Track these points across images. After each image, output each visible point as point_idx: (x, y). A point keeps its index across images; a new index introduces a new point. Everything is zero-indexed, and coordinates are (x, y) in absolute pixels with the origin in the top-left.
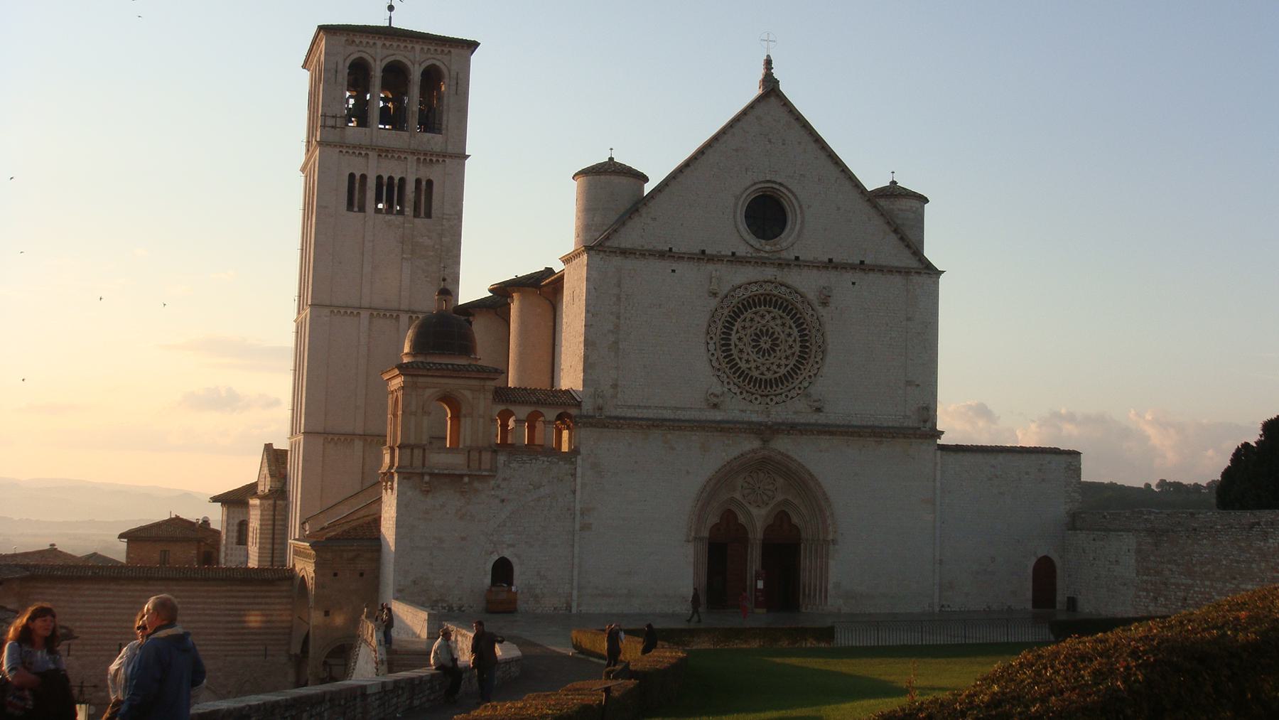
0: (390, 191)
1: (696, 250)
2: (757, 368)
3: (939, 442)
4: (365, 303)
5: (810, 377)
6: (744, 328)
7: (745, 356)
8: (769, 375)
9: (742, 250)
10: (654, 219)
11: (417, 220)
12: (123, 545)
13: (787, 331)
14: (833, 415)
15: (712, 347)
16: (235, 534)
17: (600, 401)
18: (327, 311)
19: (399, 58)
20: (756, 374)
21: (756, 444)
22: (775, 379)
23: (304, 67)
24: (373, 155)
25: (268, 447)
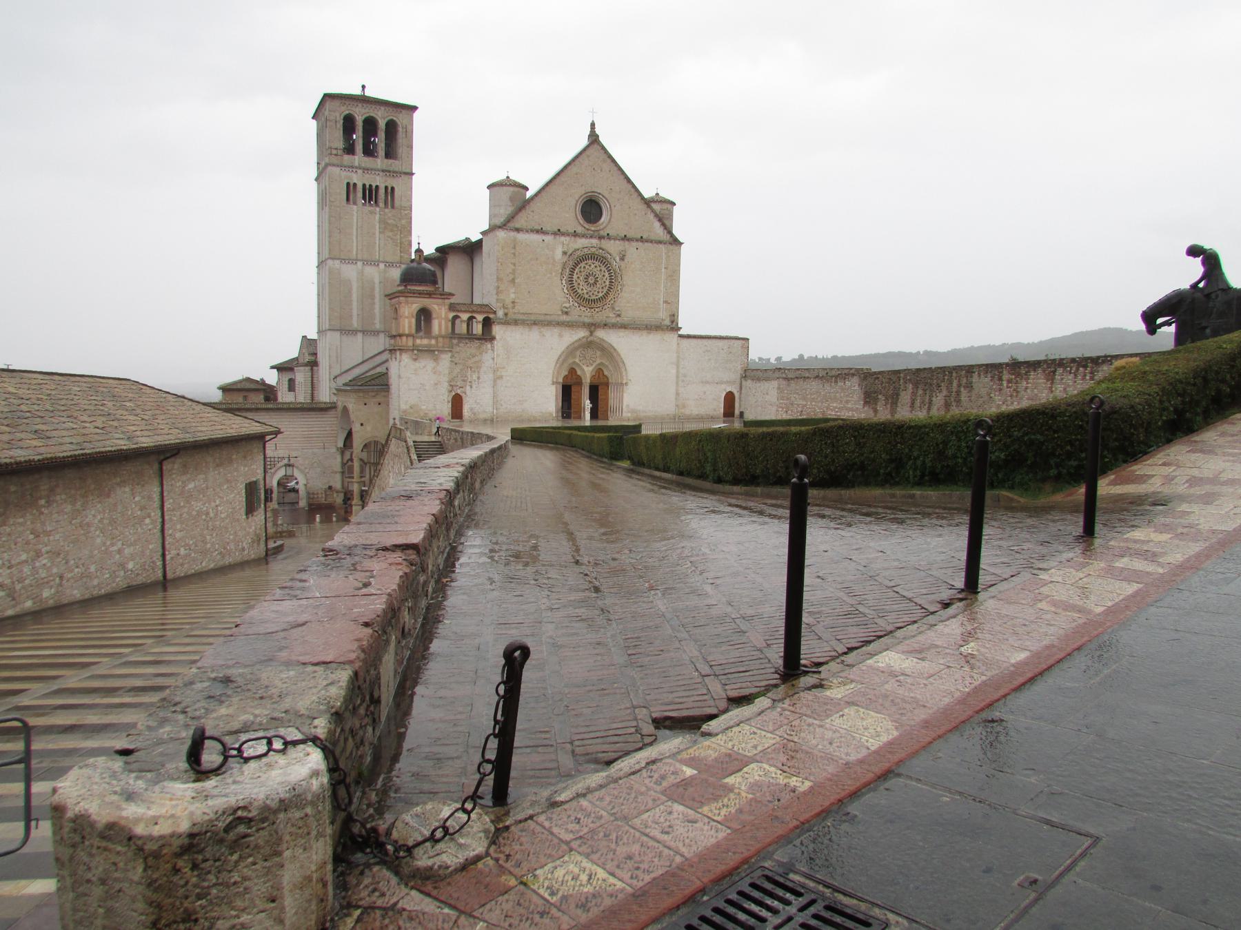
0: (370, 194)
1: (556, 230)
8: (593, 297)
9: (580, 230)
10: (533, 212)
11: (386, 210)
12: (220, 393)
14: (625, 319)
15: (564, 282)
16: (287, 386)
17: (506, 311)
19: (372, 115)
20: (586, 296)
23: (313, 118)
25: (304, 337)
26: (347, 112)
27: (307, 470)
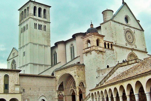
0: (40, 26)
3: (147, 54)
4: (38, 43)
8: (130, 42)
9: (126, 24)
18: (32, 44)
21: (131, 51)
23: (18, 10)
24: (38, 21)
26: (35, 6)
27: (48, 98)
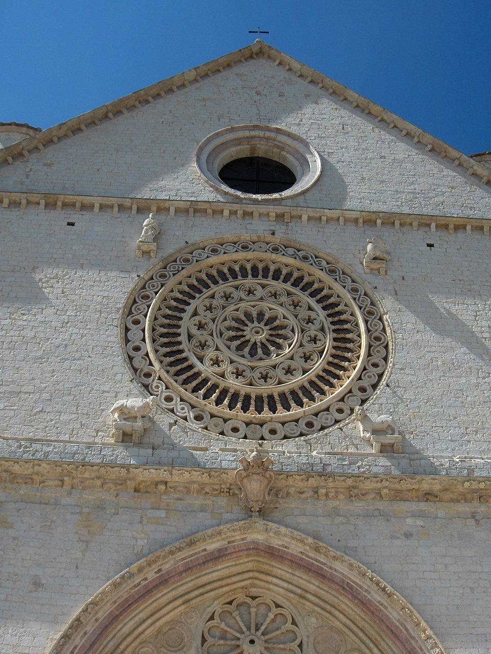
2: (238, 374)
5: (363, 390)
6: (210, 309)
7: (210, 353)
13: (303, 313)
22: (282, 395)
